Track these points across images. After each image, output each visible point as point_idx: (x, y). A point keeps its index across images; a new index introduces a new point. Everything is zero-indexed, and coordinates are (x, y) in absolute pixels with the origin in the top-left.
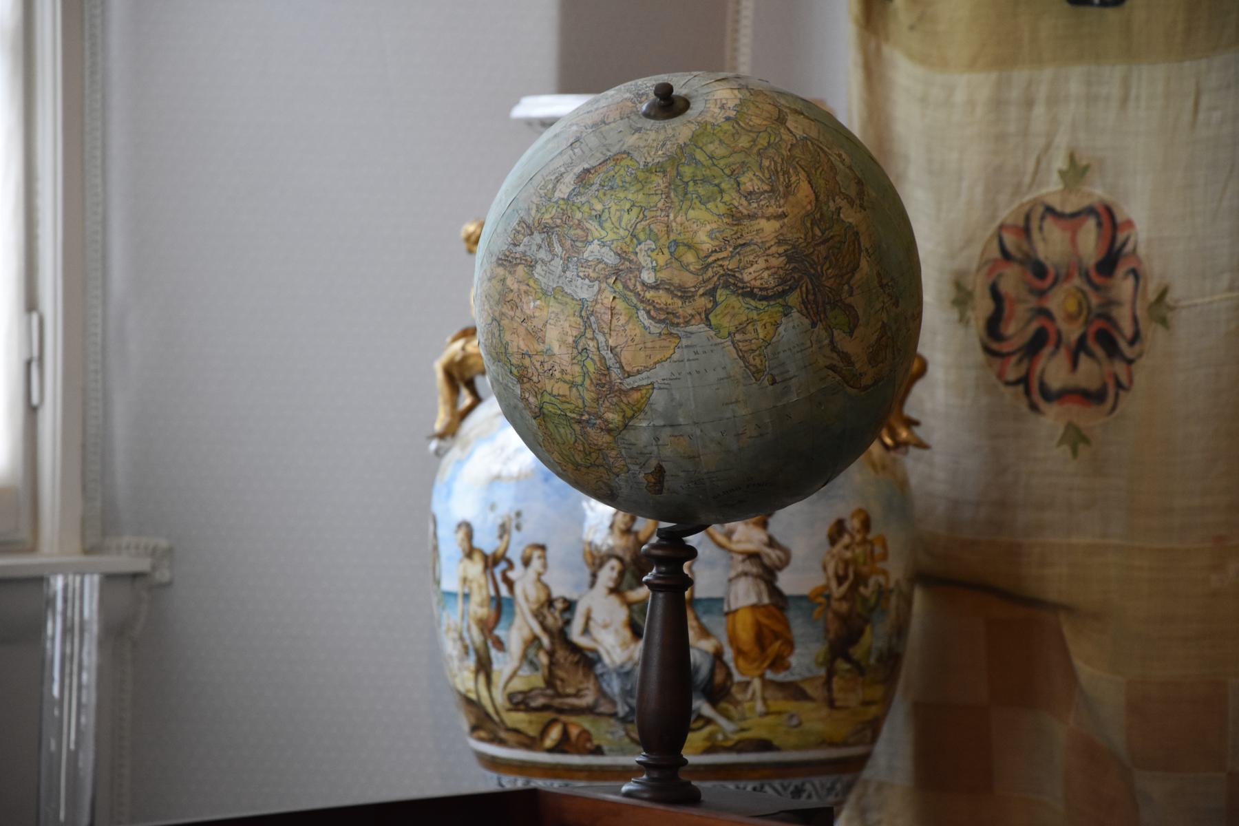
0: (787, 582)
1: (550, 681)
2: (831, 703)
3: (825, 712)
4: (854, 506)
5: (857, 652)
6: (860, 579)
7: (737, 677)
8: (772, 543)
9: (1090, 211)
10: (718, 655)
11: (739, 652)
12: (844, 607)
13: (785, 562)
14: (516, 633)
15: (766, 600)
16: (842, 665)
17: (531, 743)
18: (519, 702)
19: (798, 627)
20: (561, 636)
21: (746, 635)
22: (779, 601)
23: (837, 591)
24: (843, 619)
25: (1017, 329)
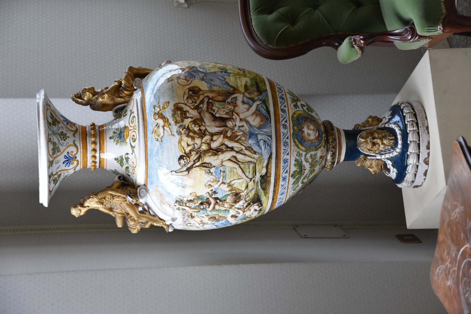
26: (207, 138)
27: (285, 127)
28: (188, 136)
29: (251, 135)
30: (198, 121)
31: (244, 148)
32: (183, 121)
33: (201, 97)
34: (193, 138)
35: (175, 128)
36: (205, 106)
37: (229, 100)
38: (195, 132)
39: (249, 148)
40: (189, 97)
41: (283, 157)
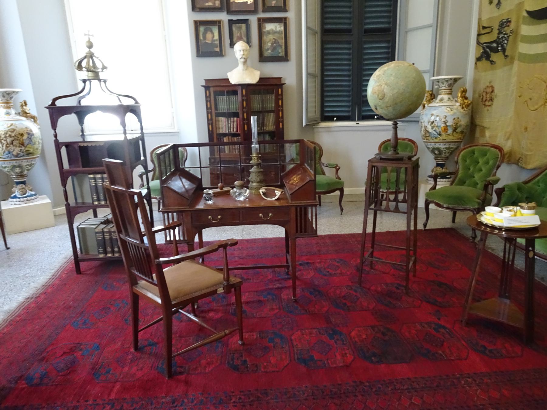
0: (448, 124)
1: (425, 134)
2: (453, 136)
3: (452, 137)
4: (457, 116)
5: (456, 131)
6: (457, 124)
7: (442, 133)
8: (446, 120)
9: (491, 86)
10: (440, 131)
11: (442, 131)
12: (455, 126)
13: (447, 122)
14: (423, 129)
15: (445, 126)
16: (455, 132)
17: (424, 140)
18: (423, 136)
19: (449, 128)
20: (426, 129)
21: (443, 129)
22: (447, 126)
23: (454, 125)
24: (455, 128)
25: (484, 99)
26: (5, 139)
27: (16, 162)
28: (5, 133)
29: (9, 152)
30: (10, 136)
31: (4, 150)
32: (10, 131)
33: (20, 137)
34: (4, 135)
35: (7, 129)
36: (16, 138)
37: (20, 145)
38: (6, 135)
39: (4, 152)
40: (19, 134)
41: (6, 162)
